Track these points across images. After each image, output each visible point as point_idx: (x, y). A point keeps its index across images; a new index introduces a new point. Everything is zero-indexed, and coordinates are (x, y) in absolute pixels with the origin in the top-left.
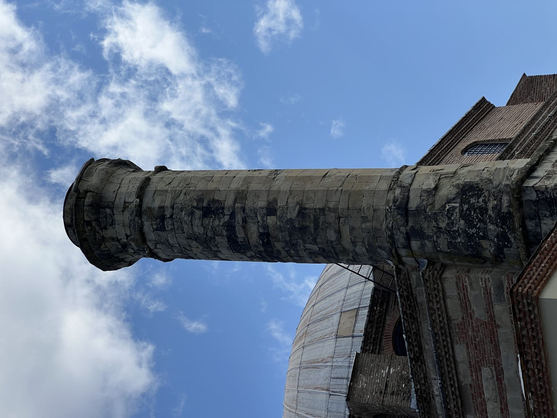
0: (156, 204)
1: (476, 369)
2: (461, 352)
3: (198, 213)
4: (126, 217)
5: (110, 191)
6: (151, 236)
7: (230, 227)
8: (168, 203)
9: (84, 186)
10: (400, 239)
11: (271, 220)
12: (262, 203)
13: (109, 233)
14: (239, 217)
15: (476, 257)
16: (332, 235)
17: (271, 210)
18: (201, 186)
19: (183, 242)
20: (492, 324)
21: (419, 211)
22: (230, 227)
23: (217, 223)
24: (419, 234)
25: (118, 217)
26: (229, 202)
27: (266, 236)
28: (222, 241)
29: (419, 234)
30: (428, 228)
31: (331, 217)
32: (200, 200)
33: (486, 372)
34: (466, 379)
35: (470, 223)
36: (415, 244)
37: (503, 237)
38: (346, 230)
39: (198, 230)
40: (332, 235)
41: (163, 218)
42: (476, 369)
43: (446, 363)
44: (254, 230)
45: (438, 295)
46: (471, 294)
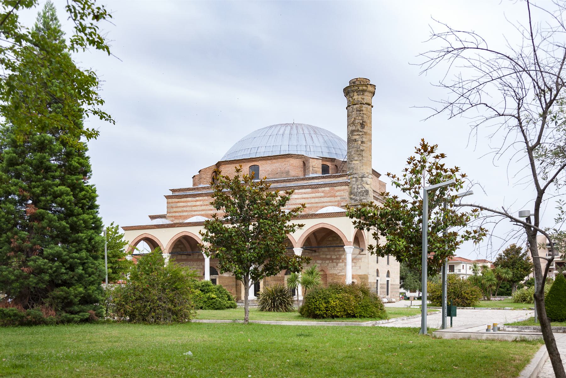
0: (364, 109)
2: (327, 189)
3: (361, 122)
4: (360, 99)
5: (366, 94)
6: (355, 107)
7: (358, 131)
8: (364, 112)
9: (369, 86)
10: (355, 176)
11: (360, 142)
12: (364, 140)
13: (356, 94)
14: (361, 133)
15: (351, 193)
16: (356, 158)
17: (362, 142)
18: (368, 121)
19: (354, 116)
20: (335, 196)
21: (362, 181)
22: (358, 131)
23: (359, 127)
24: (357, 181)
25: (360, 96)
26: (364, 130)
27: (355, 140)
28: (354, 128)
29: (357, 181)
30: (358, 183)
31: (361, 158)
32: (365, 122)
33: (322, 194)
34: (320, 190)
35: (359, 193)
36: (354, 179)
37: (356, 200)
38: (357, 162)
39: (357, 121)
40: (356, 158)
41: (360, 111)
43: (325, 185)
44: (357, 137)
45: (341, 184)
46: (342, 192)
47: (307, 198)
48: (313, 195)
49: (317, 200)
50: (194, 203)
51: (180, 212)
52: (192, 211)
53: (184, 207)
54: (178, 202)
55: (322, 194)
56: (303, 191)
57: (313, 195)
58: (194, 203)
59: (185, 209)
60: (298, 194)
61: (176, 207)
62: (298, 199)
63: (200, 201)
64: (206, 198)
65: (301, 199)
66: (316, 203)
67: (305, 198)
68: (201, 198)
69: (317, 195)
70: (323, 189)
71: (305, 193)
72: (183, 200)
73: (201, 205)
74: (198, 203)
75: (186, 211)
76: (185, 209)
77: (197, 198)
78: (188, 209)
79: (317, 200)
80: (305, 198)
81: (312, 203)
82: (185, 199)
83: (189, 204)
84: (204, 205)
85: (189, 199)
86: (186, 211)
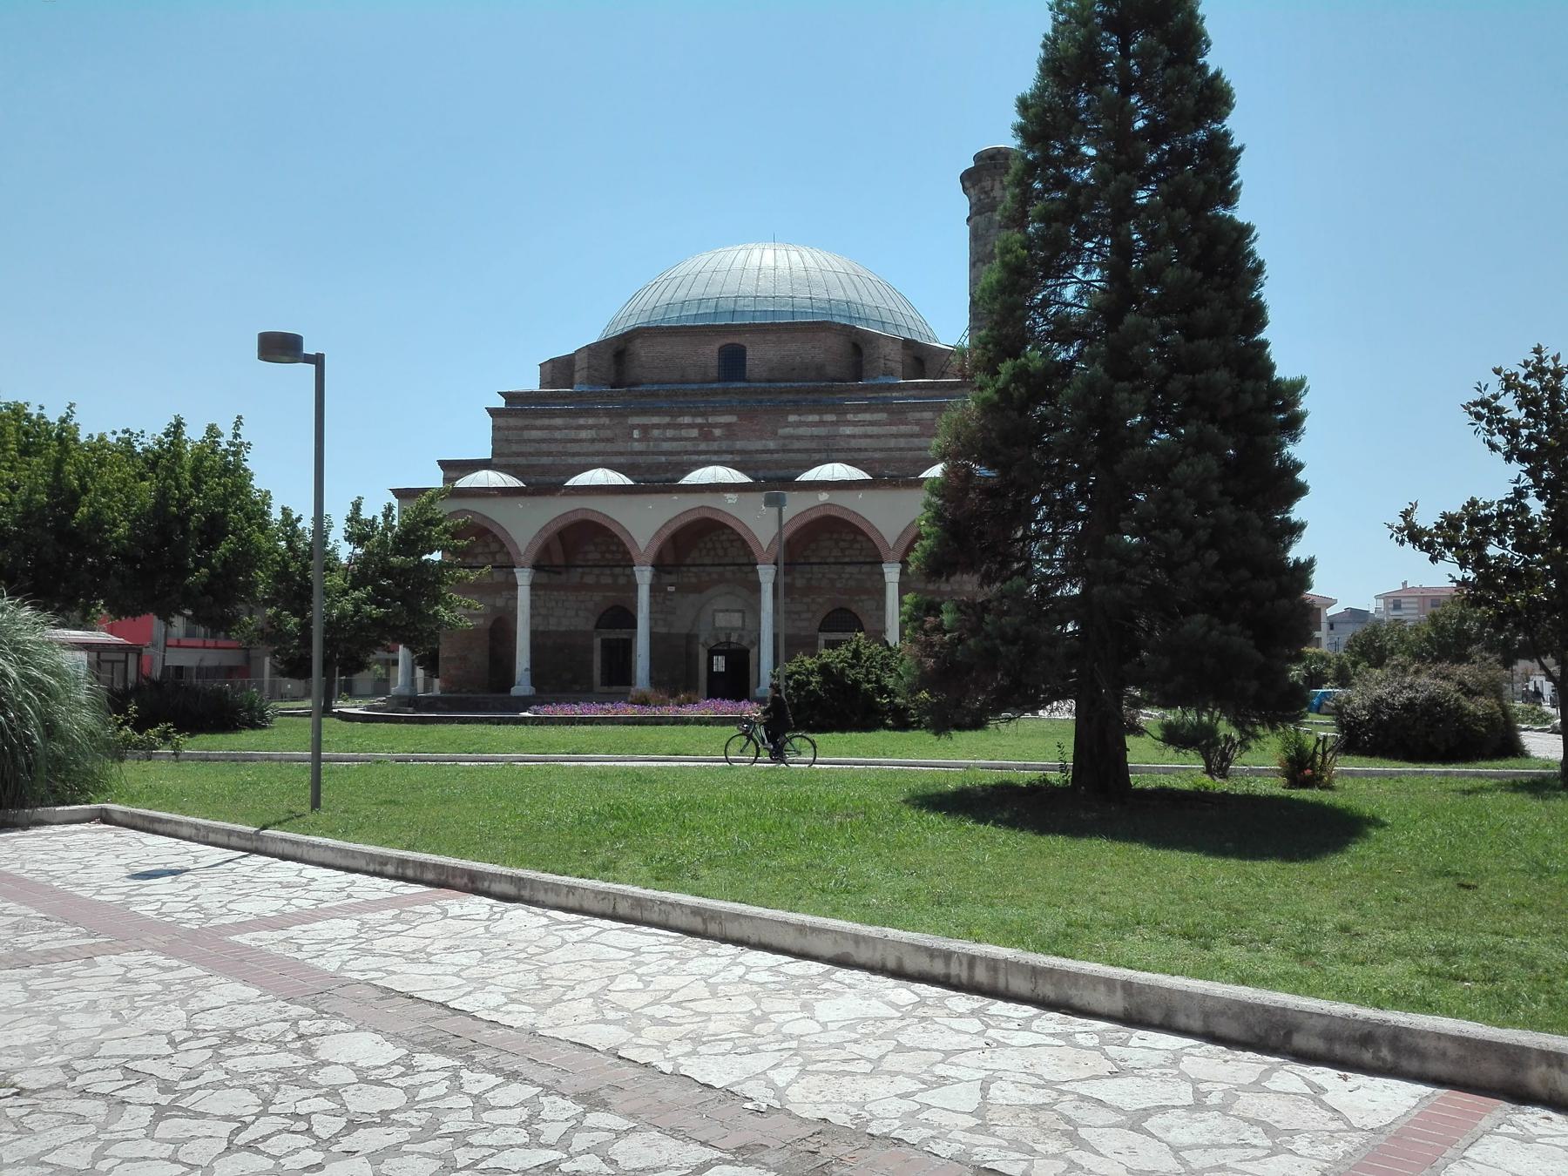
1: (918, 422)
2: (928, 415)
33: (916, 429)
42: (918, 422)
47: (878, 436)
48: (894, 429)
49: (902, 443)
50: (572, 434)
51: (530, 454)
52: (566, 454)
53: (543, 441)
54: (527, 428)
55: (916, 429)
56: (867, 417)
57: (894, 429)
58: (572, 434)
59: (544, 447)
60: (855, 424)
61: (518, 442)
62: (854, 436)
63: (591, 427)
64: (605, 421)
65: (860, 437)
66: (901, 449)
67: (871, 437)
68: (591, 421)
69: (903, 429)
70: (918, 415)
71: (871, 423)
72: (539, 422)
73: (593, 441)
74: (583, 434)
75: (549, 454)
76: (544, 447)
77: (582, 421)
78: (554, 448)
79: (902, 443)
80: (871, 437)
81: (890, 449)
82: (546, 422)
83: (558, 435)
84: (602, 440)
85: (558, 421)
86: (549, 454)
